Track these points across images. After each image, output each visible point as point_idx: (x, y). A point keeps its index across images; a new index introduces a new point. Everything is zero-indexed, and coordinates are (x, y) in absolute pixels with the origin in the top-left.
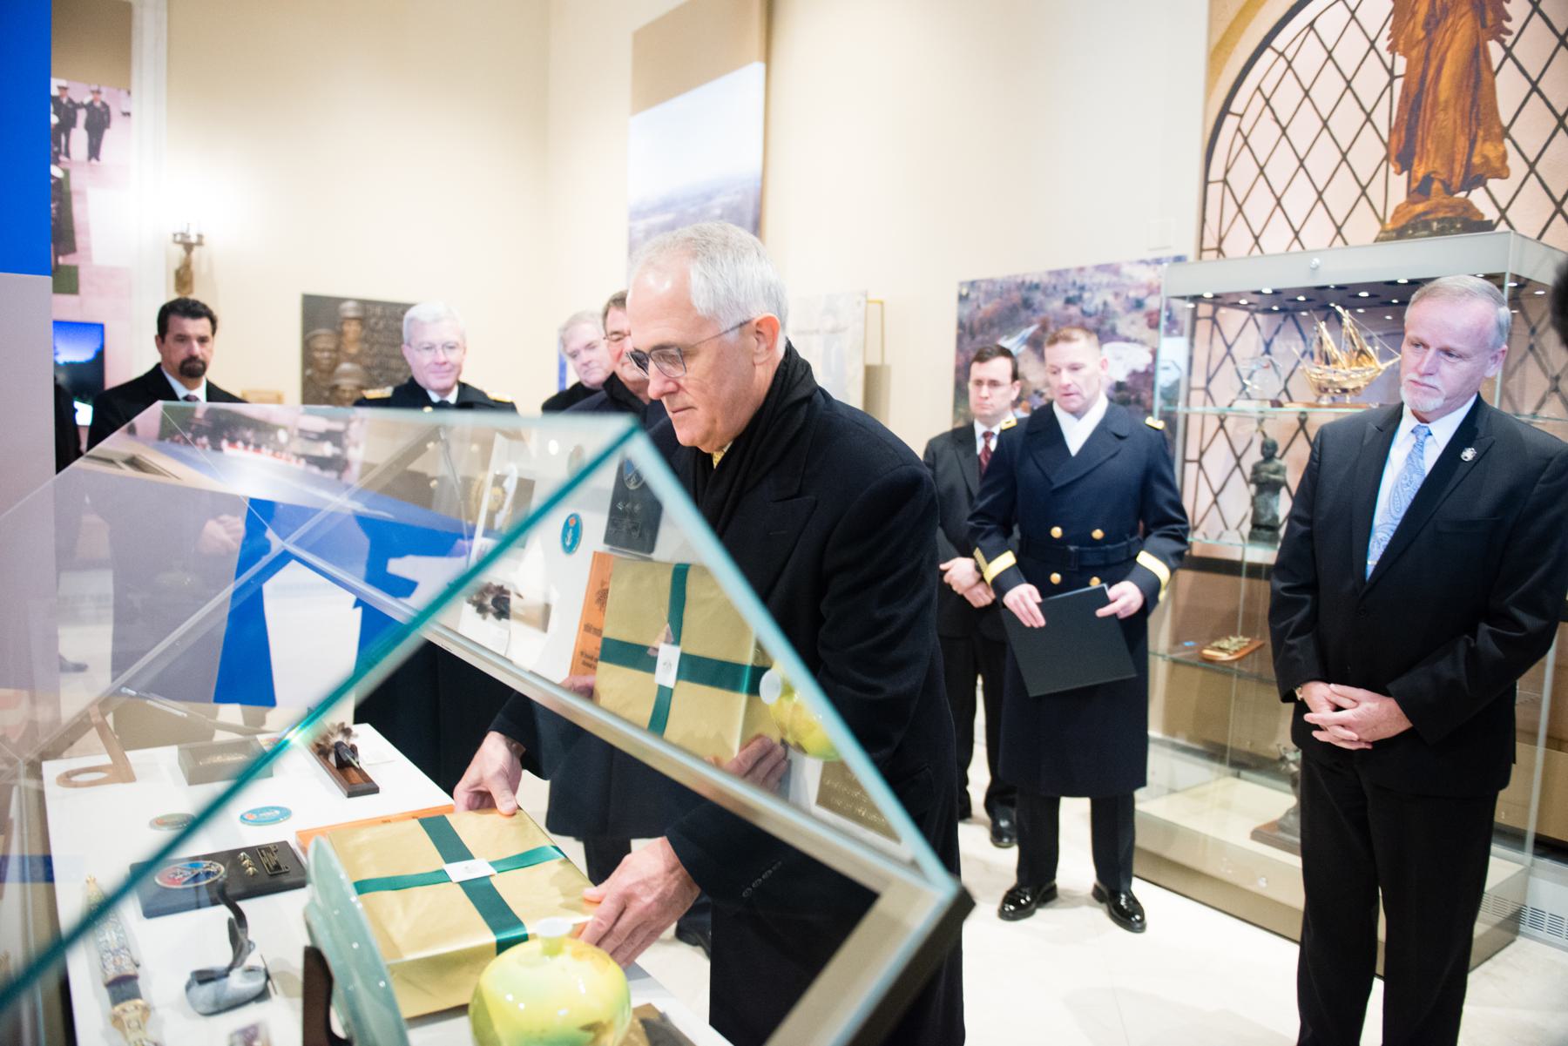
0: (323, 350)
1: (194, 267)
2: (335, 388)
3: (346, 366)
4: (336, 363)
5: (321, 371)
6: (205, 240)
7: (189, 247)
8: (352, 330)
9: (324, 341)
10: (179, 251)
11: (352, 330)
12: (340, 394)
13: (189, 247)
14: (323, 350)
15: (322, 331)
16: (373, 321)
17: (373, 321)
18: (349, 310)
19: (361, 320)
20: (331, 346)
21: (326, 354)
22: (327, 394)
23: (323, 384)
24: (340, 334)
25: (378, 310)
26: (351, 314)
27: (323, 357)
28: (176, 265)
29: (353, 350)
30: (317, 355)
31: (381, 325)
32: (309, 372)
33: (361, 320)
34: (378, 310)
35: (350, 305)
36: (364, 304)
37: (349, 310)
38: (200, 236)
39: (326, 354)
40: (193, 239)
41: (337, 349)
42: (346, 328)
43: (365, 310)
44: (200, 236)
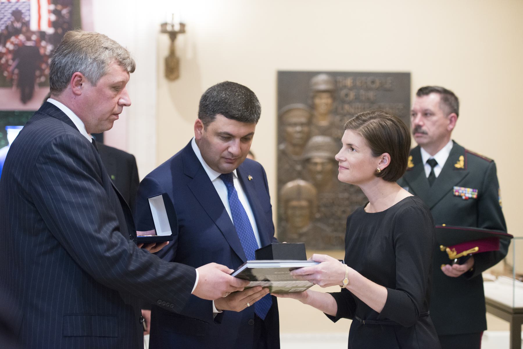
0: (295, 124)
1: (179, 53)
2: (308, 161)
3: (318, 139)
4: (308, 137)
5: (294, 145)
6: (187, 28)
7: (173, 35)
8: (323, 102)
9: (298, 115)
10: (165, 39)
11: (323, 102)
12: (312, 167)
13: (173, 35)
14: (295, 124)
15: (300, 106)
16: (343, 93)
17: (343, 93)
18: (322, 83)
19: (332, 93)
20: (303, 120)
21: (298, 128)
22: (299, 167)
23: (296, 158)
24: (313, 107)
25: (349, 82)
26: (323, 87)
27: (295, 131)
28: (165, 52)
29: (324, 123)
30: (290, 129)
31: (352, 95)
32: (282, 147)
33: (332, 93)
34: (349, 82)
35: (322, 78)
36: (335, 76)
37: (322, 83)
38: (182, 25)
39: (298, 128)
40: (177, 28)
41: (309, 122)
42: (317, 101)
43: (335, 82)
44: (182, 25)
